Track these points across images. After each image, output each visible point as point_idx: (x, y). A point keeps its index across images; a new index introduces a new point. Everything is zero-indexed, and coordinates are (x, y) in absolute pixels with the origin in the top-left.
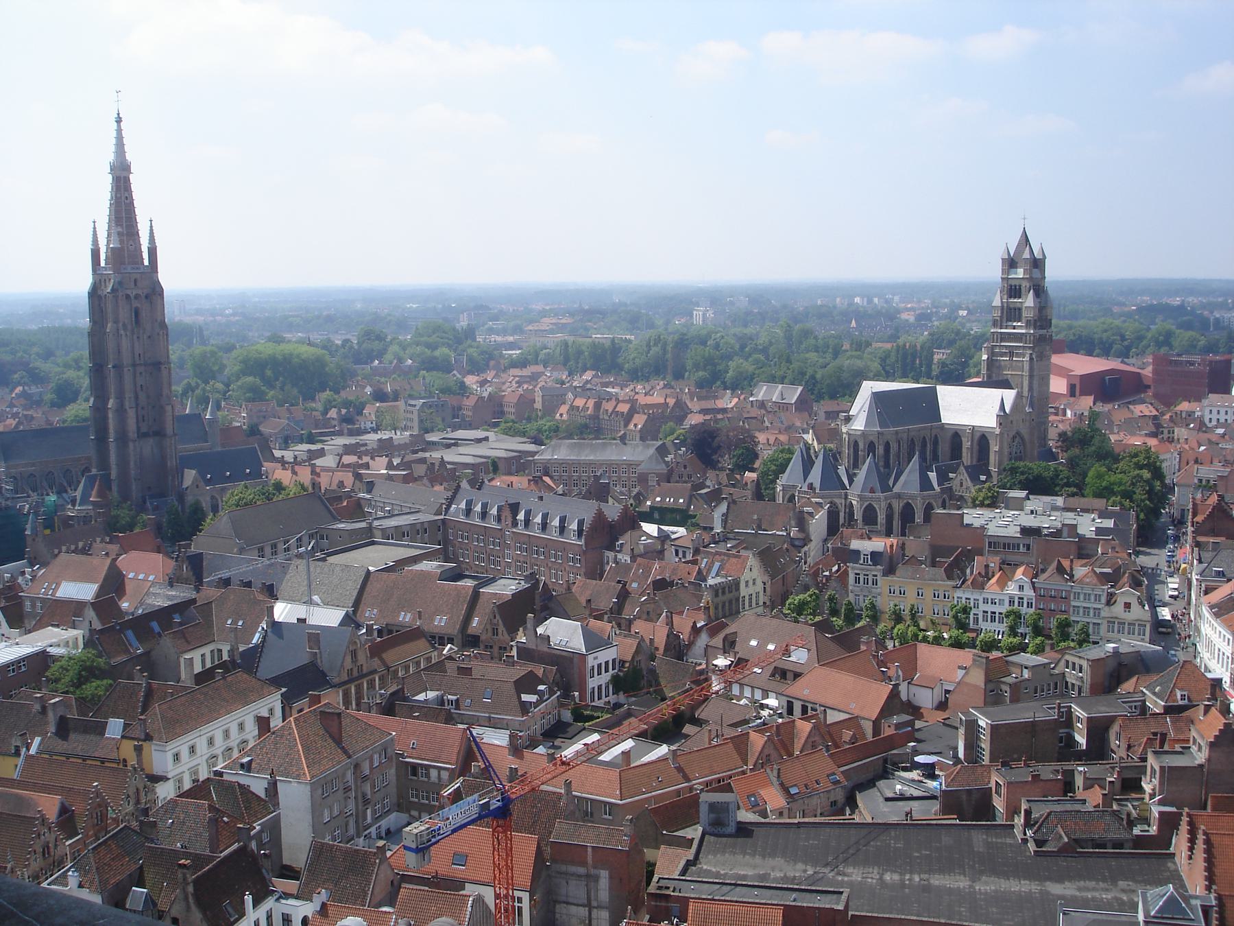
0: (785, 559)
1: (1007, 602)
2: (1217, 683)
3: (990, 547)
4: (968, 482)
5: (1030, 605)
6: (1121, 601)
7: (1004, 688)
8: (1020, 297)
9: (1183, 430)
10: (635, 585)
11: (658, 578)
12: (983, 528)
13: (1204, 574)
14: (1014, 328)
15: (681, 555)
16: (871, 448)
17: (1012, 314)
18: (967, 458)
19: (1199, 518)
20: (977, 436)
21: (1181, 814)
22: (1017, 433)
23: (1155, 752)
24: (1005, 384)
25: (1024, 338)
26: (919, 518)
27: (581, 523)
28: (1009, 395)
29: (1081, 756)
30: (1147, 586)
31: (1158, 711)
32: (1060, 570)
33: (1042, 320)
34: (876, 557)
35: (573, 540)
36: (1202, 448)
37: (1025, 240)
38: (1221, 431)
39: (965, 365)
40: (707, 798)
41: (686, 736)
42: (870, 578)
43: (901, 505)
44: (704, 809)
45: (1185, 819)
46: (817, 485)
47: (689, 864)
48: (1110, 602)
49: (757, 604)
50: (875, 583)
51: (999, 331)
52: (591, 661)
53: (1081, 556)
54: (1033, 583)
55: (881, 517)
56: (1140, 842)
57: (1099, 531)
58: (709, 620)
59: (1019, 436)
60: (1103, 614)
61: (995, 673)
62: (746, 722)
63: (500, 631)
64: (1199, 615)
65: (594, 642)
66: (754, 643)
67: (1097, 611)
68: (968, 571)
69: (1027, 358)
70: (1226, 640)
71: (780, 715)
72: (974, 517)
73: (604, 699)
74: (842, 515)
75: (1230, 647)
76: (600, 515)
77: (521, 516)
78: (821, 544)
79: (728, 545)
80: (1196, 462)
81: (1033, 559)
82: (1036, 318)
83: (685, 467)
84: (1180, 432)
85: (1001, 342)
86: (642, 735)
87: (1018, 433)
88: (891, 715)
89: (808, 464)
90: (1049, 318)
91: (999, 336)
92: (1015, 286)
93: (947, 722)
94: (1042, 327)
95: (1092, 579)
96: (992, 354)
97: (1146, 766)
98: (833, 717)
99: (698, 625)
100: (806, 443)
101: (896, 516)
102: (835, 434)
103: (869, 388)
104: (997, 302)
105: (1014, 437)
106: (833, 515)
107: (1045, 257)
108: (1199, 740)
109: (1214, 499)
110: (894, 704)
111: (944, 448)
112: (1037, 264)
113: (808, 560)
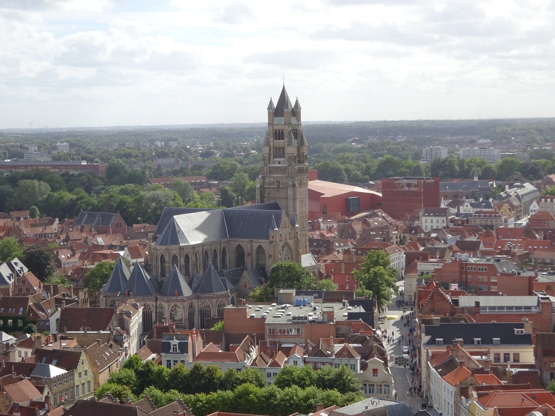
0: (109, 352)
8: (283, 139)
14: (279, 163)
15: (23, 355)
16: (175, 259)
22: (285, 243)
37: (283, 97)
38: (434, 235)
49: (89, 391)
57: (351, 316)
59: (287, 245)
74: (154, 314)
75: (453, 398)
87: (286, 243)
90: (305, 154)
92: (279, 131)
94: (300, 162)
101: (196, 313)
105: (283, 247)
111: (230, 257)
112: (296, 112)
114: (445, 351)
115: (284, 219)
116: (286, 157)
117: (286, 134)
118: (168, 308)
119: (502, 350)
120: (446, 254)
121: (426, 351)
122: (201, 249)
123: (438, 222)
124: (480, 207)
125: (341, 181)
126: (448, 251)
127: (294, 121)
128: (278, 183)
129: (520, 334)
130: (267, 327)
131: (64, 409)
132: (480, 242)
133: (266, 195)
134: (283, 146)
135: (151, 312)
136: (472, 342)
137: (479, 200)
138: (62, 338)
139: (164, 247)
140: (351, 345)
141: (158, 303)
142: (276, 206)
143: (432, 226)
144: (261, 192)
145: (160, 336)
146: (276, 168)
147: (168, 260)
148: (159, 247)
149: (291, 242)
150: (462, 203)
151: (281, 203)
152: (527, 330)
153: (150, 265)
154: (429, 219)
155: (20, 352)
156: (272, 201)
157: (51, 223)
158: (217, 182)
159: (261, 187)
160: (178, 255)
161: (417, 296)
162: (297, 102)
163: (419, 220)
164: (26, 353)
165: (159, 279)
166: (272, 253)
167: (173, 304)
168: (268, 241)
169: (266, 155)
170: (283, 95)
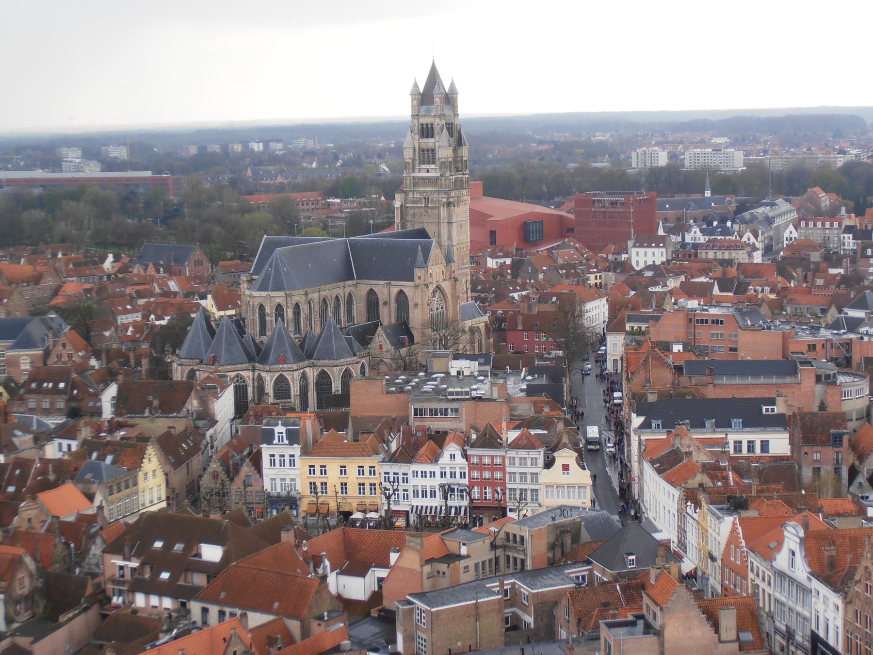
0: (188, 444)
1: (438, 474)
2: (666, 545)
3: (416, 414)
4: (388, 346)
5: (462, 475)
6: (559, 461)
8: (432, 137)
10: (11, 489)
14: (428, 171)
15: (65, 449)
18: (387, 315)
22: (437, 287)
25: (439, 182)
26: (336, 386)
31: (606, 579)
37: (433, 77)
38: (649, 274)
42: (287, 459)
43: (316, 374)
48: (549, 464)
50: (292, 463)
51: (413, 175)
55: (295, 390)
66: (158, 544)
67: (535, 475)
70: (671, 495)
74: (250, 390)
78: (228, 424)
80: (627, 307)
82: (450, 159)
83: (64, 345)
85: (414, 186)
87: (438, 288)
90: (464, 158)
91: (412, 180)
92: (427, 125)
99: (93, 530)
100: (205, 310)
105: (434, 292)
112: (450, 99)
113: (215, 443)
114: (665, 437)
115: (435, 252)
116: (437, 162)
117: (437, 129)
118: (271, 380)
119: (745, 437)
120: (667, 301)
121: (637, 438)
122: (316, 295)
123: (655, 256)
124: (714, 235)
125: (517, 198)
126: (668, 296)
127: (448, 112)
128: (427, 199)
129: (770, 413)
130: (412, 408)
131: (126, 524)
132: (714, 283)
133: (409, 218)
134: (433, 147)
135: (246, 386)
136: (703, 426)
137: (712, 224)
138: (121, 426)
139: (264, 294)
140: (533, 432)
141: (256, 373)
142: (422, 234)
143: (646, 261)
144: (402, 213)
145: (258, 418)
146: (423, 179)
147: (269, 312)
148: (256, 293)
149: (446, 286)
150: (688, 229)
151: (431, 230)
152: (779, 408)
153: (244, 319)
154: (642, 251)
155: (60, 444)
156: (417, 227)
157: (103, 259)
158: (338, 201)
159: (401, 206)
160: (283, 303)
161: (625, 359)
162: (452, 84)
163: (627, 253)
164: (69, 446)
165: (258, 339)
166: (419, 302)
167: (277, 375)
168: (412, 284)
169: (407, 160)
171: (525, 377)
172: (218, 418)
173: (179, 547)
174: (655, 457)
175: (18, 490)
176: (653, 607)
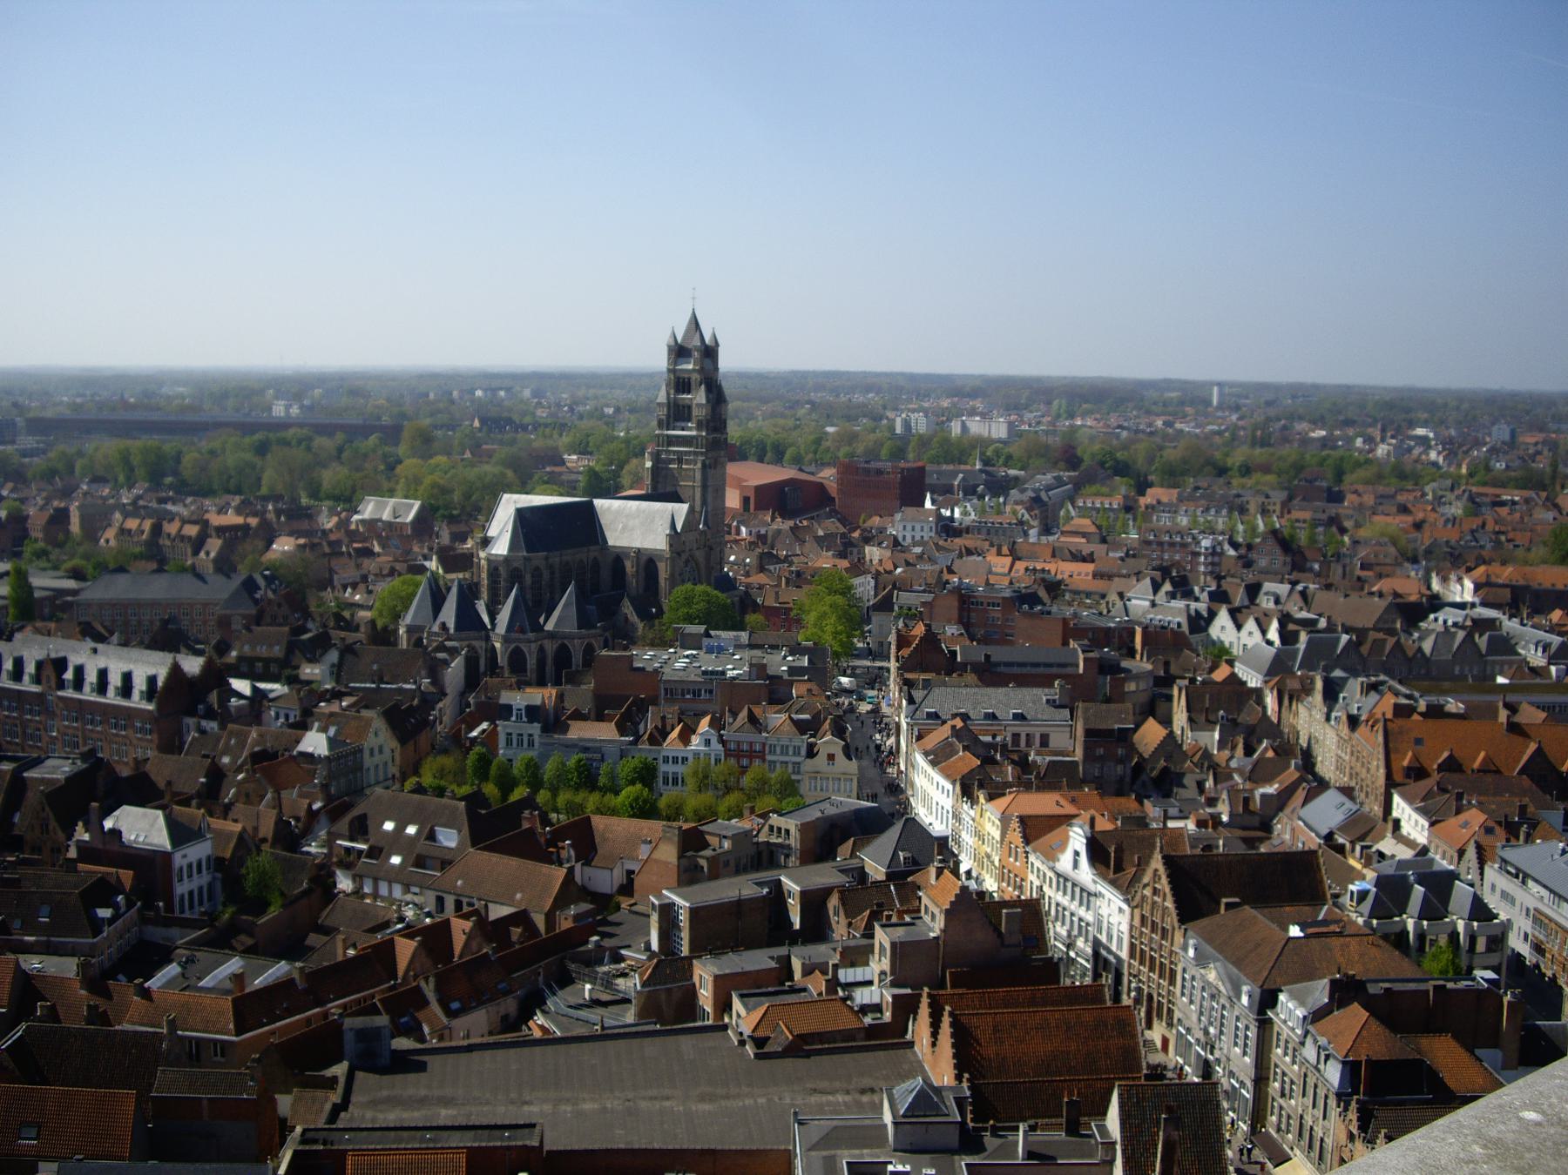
7: (703, 863)
8: (689, 392)
9: (875, 549)
10: (226, 760)
11: (256, 749)
12: (656, 671)
13: (917, 716)
17: (678, 413)
19: (906, 652)
20: (643, 559)
21: (920, 995)
23: (883, 926)
24: (675, 498)
26: (577, 658)
27: (152, 680)
28: (681, 509)
29: (795, 938)
30: (851, 733)
32: (752, 719)
33: (716, 422)
34: (533, 713)
35: (137, 701)
36: (899, 570)
39: (616, 475)
40: (349, 1023)
41: (311, 949)
44: (349, 1038)
45: (925, 1001)
46: (451, 625)
47: (337, 1110)
52: (179, 860)
53: (772, 702)
54: (721, 736)
55: (531, 662)
56: (874, 1031)
57: (793, 671)
58: (329, 799)
60: (804, 768)
61: (692, 842)
62: (387, 924)
63: (51, 828)
64: (911, 764)
65: (180, 833)
66: (389, 826)
68: (642, 726)
69: (699, 465)
71: (429, 915)
72: (646, 657)
73: (197, 909)
74: (482, 662)
76: (176, 670)
77: (69, 675)
79: (344, 704)
81: (717, 708)
84: (873, 553)
86: (248, 951)
88: (567, 906)
89: (438, 600)
93: (634, 908)
95: (788, 727)
96: (656, 457)
97: (873, 945)
98: (498, 912)
101: (549, 661)
102: (465, 562)
103: (508, 506)
104: (662, 397)
105: (687, 562)
106: (471, 664)
107: (717, 345)
108: (932, 908)
109: (919, 630)
110: (570, 891)
113: (444, 719)
116: (694, 419)
122: (557, 559)
167: (513, 646)
170: (695, 324)
171: (785, 657)
172: (448, 691)
173: (411, 830)
174: (929, 747)
175: (234, 761)
176: (932, 908)
